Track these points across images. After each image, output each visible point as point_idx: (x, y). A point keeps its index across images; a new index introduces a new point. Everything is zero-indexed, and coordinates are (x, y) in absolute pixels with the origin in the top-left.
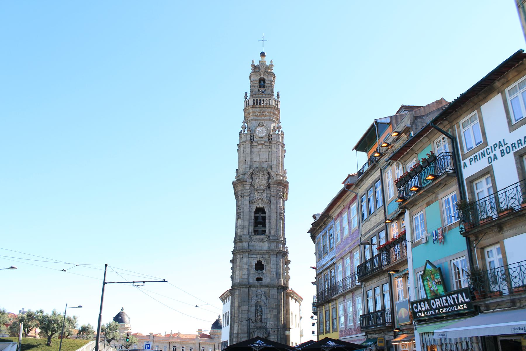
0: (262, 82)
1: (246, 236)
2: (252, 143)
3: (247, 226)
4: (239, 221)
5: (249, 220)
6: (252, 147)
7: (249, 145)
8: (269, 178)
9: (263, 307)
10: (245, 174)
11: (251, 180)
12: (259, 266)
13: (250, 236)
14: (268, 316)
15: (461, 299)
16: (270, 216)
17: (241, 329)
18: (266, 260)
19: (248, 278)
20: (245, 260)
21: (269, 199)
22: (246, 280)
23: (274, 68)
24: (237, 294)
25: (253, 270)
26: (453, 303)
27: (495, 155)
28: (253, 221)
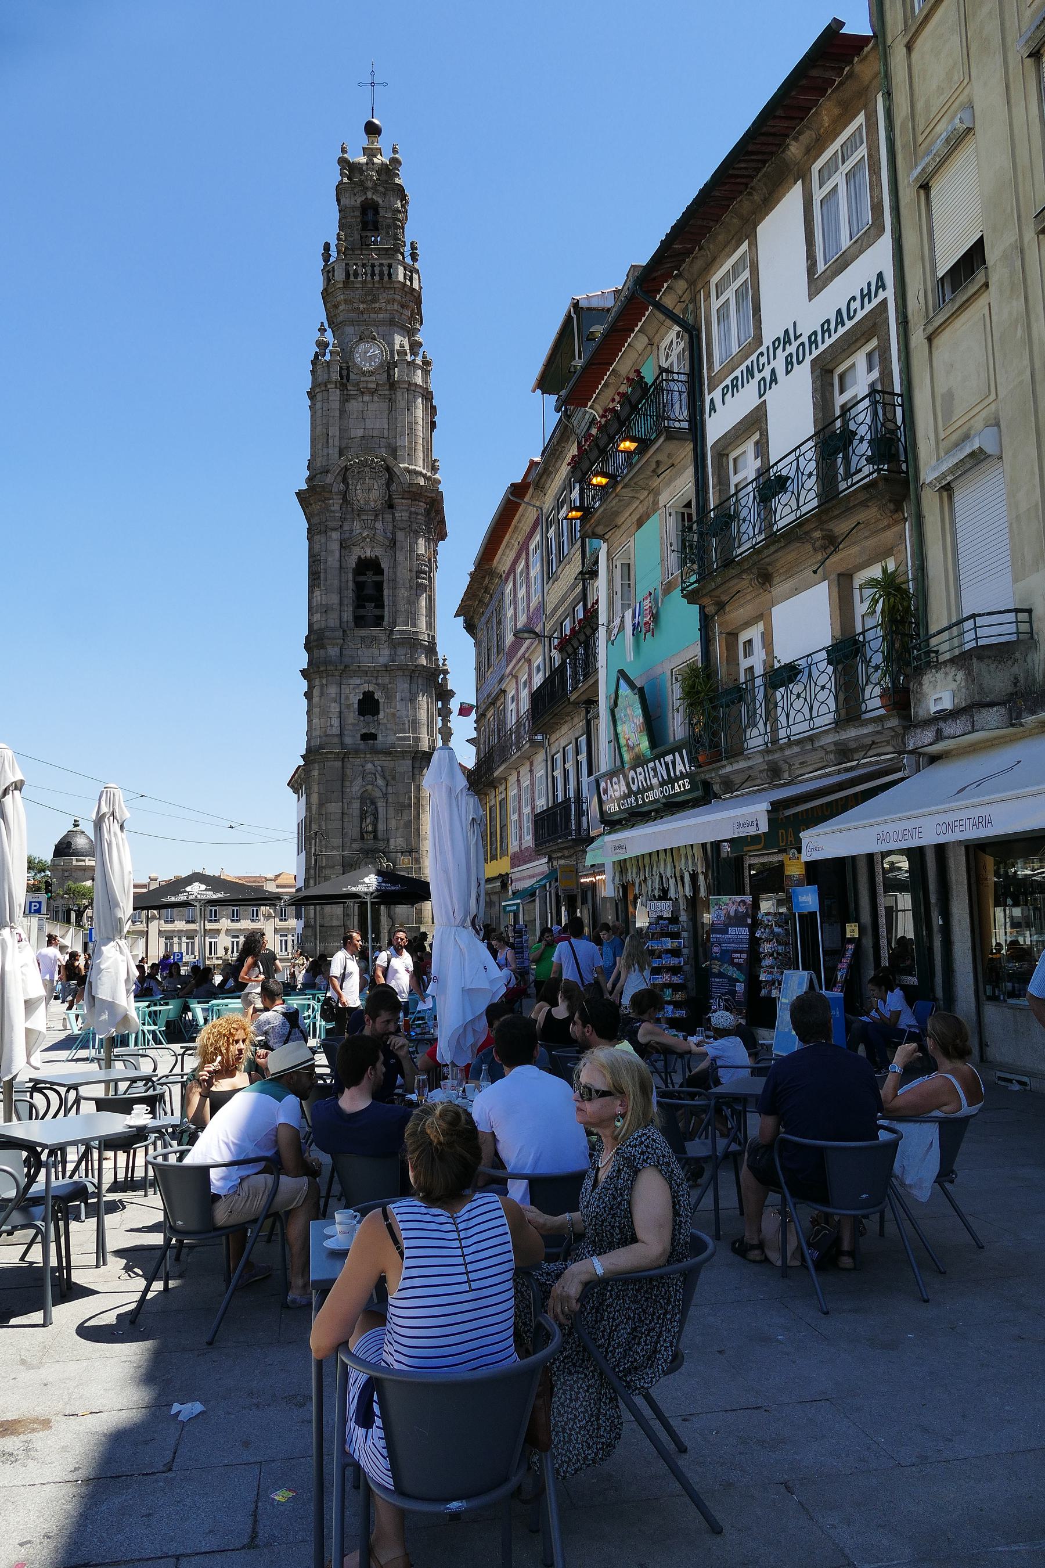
0: (370, 214)
1: (333, 630)
3: (336, 607)
6: (345, 398)
7: (335, 395)
9: (379, 804)
12: (368, 706)
13: (344, 631)
14: (393, 823)
15: (680, 767)
16: (394, 580)
18: (384, 687)
20: (333, 690)
21: (389, 535)
22: (336, 740)
23: (402, 171)
24: (315, 773)
26: (666, 777)
27: (773, 371)
28: (350, 593)
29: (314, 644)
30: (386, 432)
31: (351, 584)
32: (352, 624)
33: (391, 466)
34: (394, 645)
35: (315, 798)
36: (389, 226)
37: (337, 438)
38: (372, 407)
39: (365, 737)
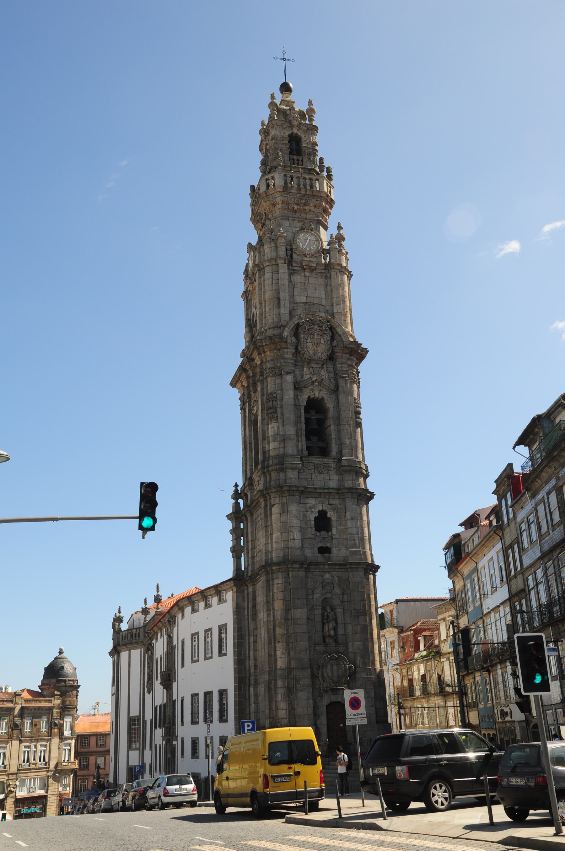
1: (293, 456)
2: (290, 261)
5: (297, 423)
6: (292, 272)
7: (284, 269)
9: (338, 611)
11: (294, 340)
12: (323, 522)
13: (301, 458)
14: (350, 627)
18: (335, 509)
20: (293, 508)
22: (298, 552)
29: (274, 467)
30: (324, 301)
31: (303, 419)
32: (306, 453)
33: (335, 326)
36: (310, 154)
37: (287, 302)
38: (312, 280)
39: (324, 550)
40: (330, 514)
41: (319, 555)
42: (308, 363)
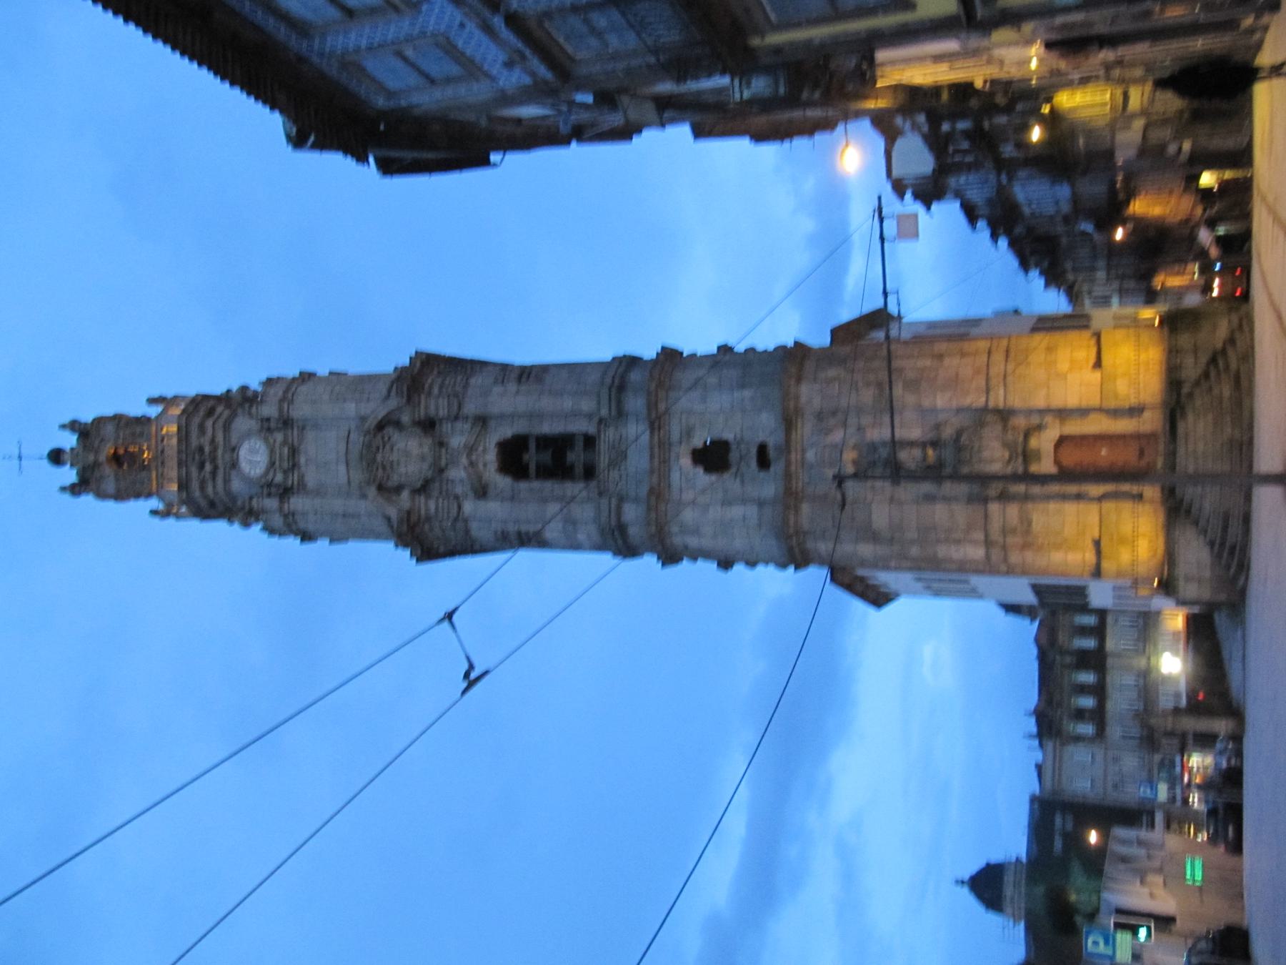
2: (285, 492)
4: (549, 534)
5: (544, 501)
6: (301, 487)
7: (297, 503)
8: (398, 425)
10: (389, 519)
11: (405, 494)
12: (714, 457)
17: (969, 528)
19: (761, 504)
21: (467, 426)
25: (728, 481)
28: (548, 486)
31: (536, 484)
32: (593, 484)
34: (620, 414)
35: (866, 550)
36: (133, 434)
39: (763, 460)
40: (698, 442)
41: (772, 469)
42: (441, 471)
